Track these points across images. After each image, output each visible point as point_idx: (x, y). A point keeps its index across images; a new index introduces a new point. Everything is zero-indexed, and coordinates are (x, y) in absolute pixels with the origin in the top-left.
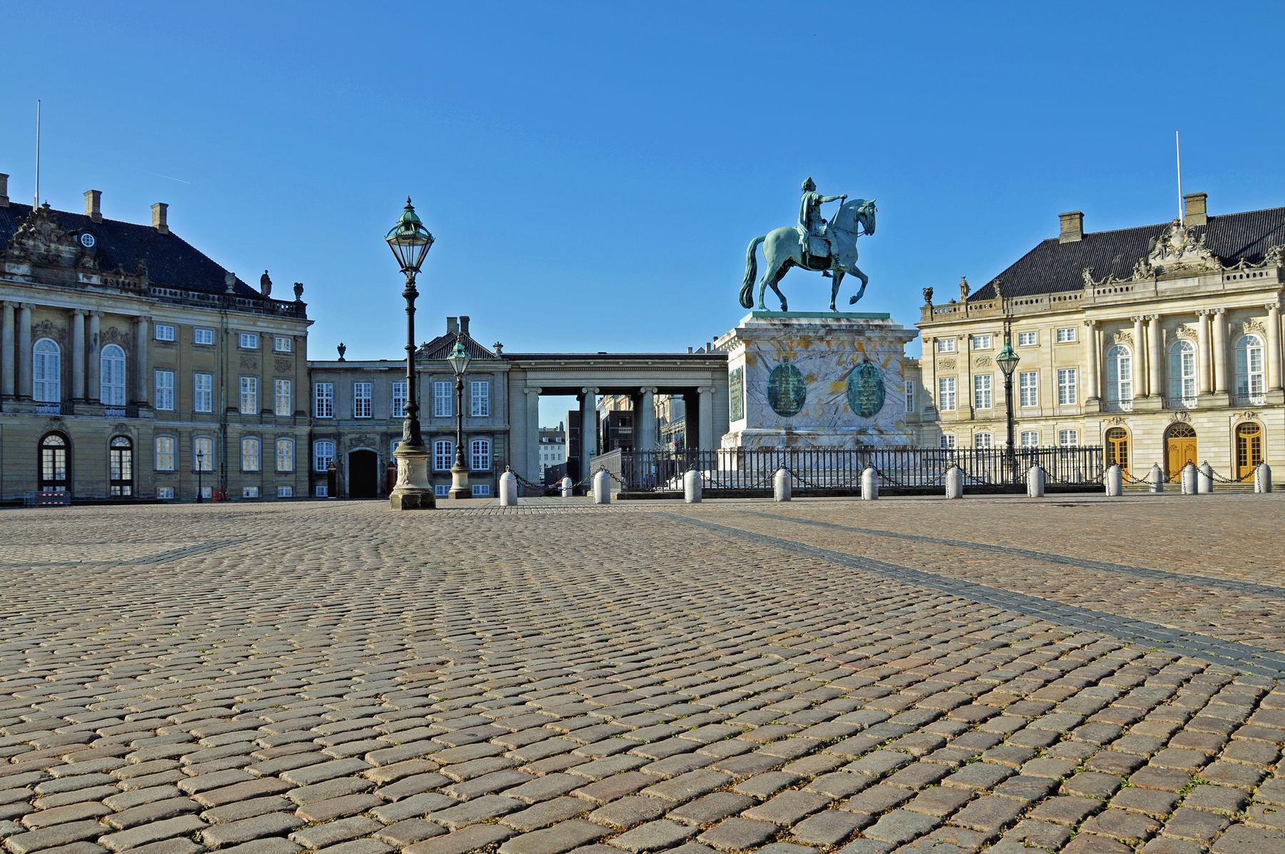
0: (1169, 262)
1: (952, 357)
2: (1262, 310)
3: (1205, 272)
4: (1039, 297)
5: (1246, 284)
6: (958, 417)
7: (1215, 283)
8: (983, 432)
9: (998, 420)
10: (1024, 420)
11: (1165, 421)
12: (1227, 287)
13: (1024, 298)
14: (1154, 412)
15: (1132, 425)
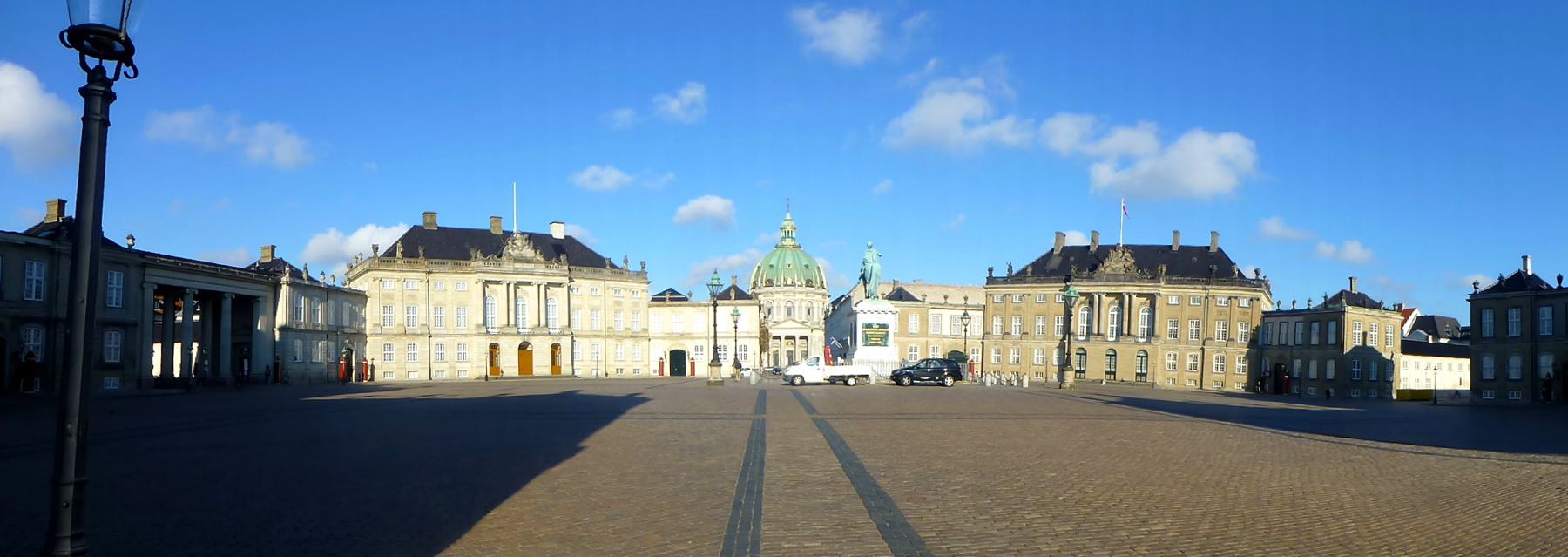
0: (515, 253)
1: (391, 292)
2: (560, 285)
3: (537, 262)
4: (445, 261)
5: (555, 271)
6: (395, 332)
7: (542, 268)
8: (413, 342)
9: (422, 335)
10: (437, 336)
11: (519, 341)
12: (548, 271)
13: (437, 260)
14: (514, 335)
15: (504, 343)
